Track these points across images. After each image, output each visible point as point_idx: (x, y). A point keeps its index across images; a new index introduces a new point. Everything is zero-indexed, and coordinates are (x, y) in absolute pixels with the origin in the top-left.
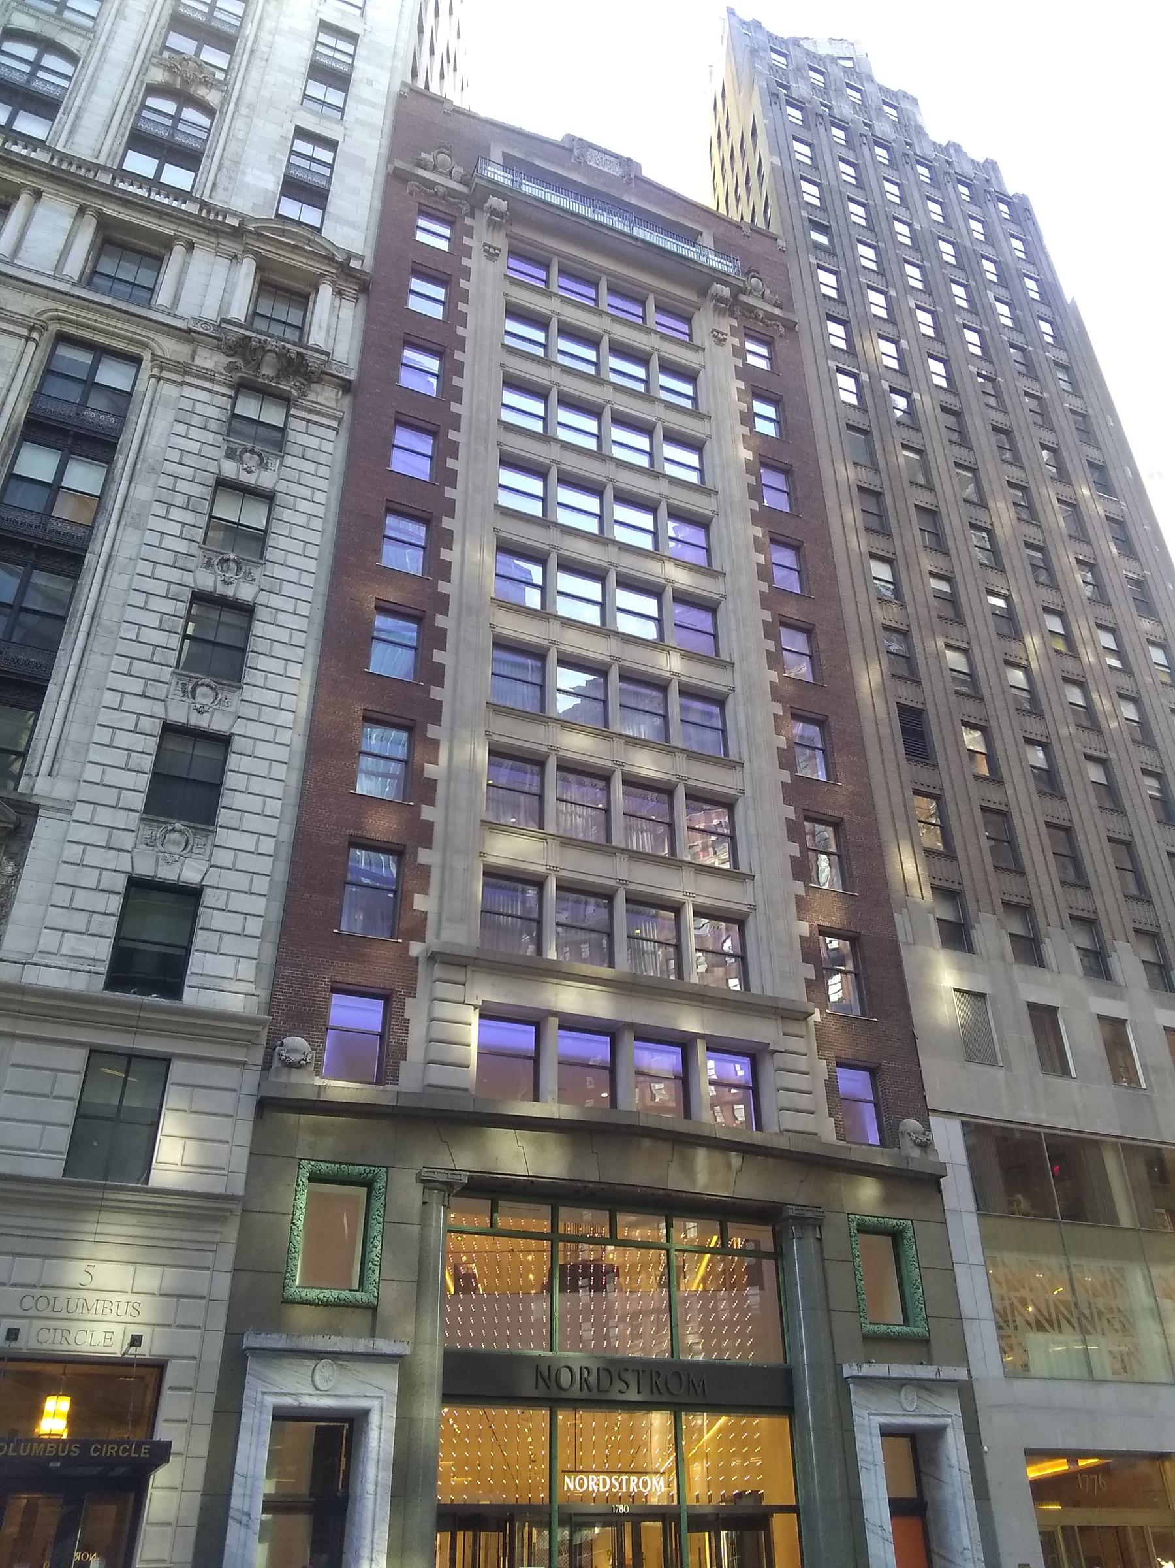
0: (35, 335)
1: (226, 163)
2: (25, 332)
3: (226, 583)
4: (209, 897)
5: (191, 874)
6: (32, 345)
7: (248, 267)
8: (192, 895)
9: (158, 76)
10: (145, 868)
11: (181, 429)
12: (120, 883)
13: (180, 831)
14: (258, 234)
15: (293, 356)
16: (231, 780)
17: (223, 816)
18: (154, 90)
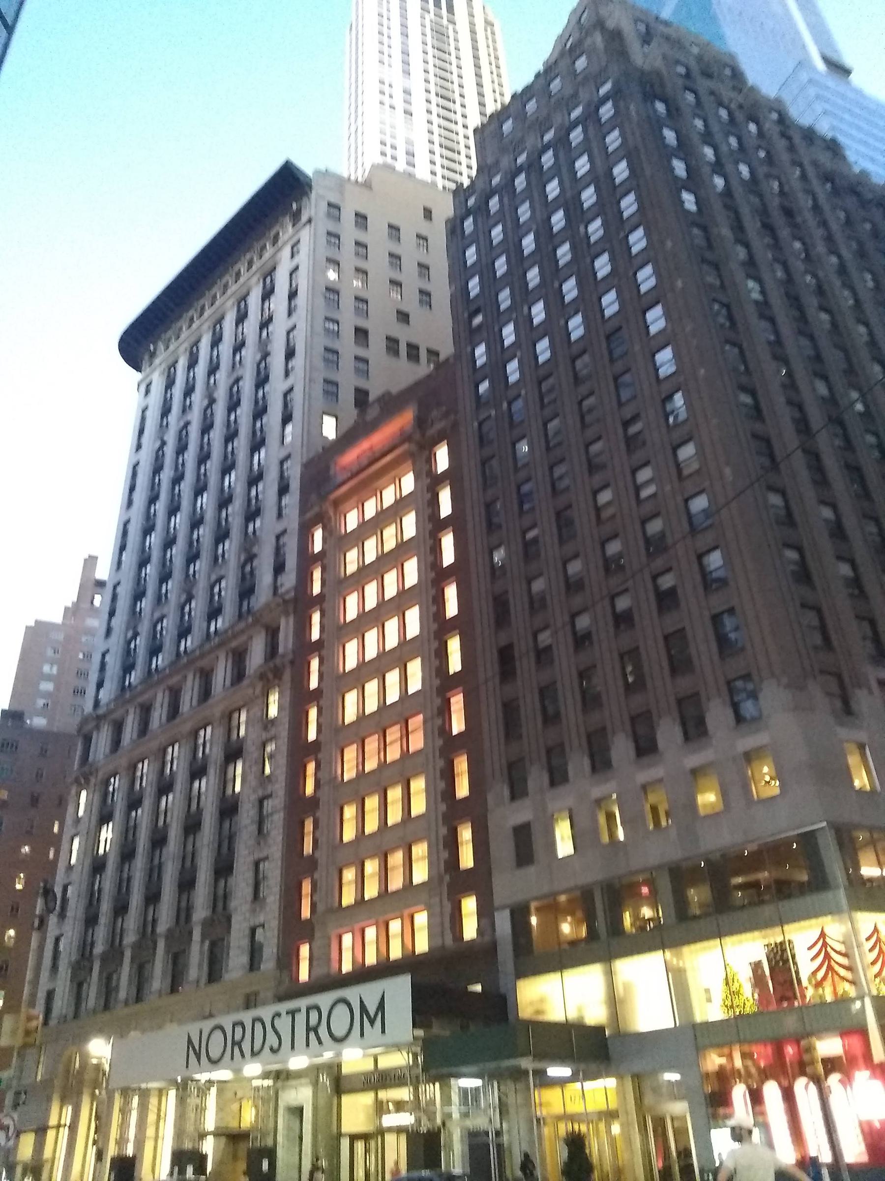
7: (263, 634)
9: (243, 558)
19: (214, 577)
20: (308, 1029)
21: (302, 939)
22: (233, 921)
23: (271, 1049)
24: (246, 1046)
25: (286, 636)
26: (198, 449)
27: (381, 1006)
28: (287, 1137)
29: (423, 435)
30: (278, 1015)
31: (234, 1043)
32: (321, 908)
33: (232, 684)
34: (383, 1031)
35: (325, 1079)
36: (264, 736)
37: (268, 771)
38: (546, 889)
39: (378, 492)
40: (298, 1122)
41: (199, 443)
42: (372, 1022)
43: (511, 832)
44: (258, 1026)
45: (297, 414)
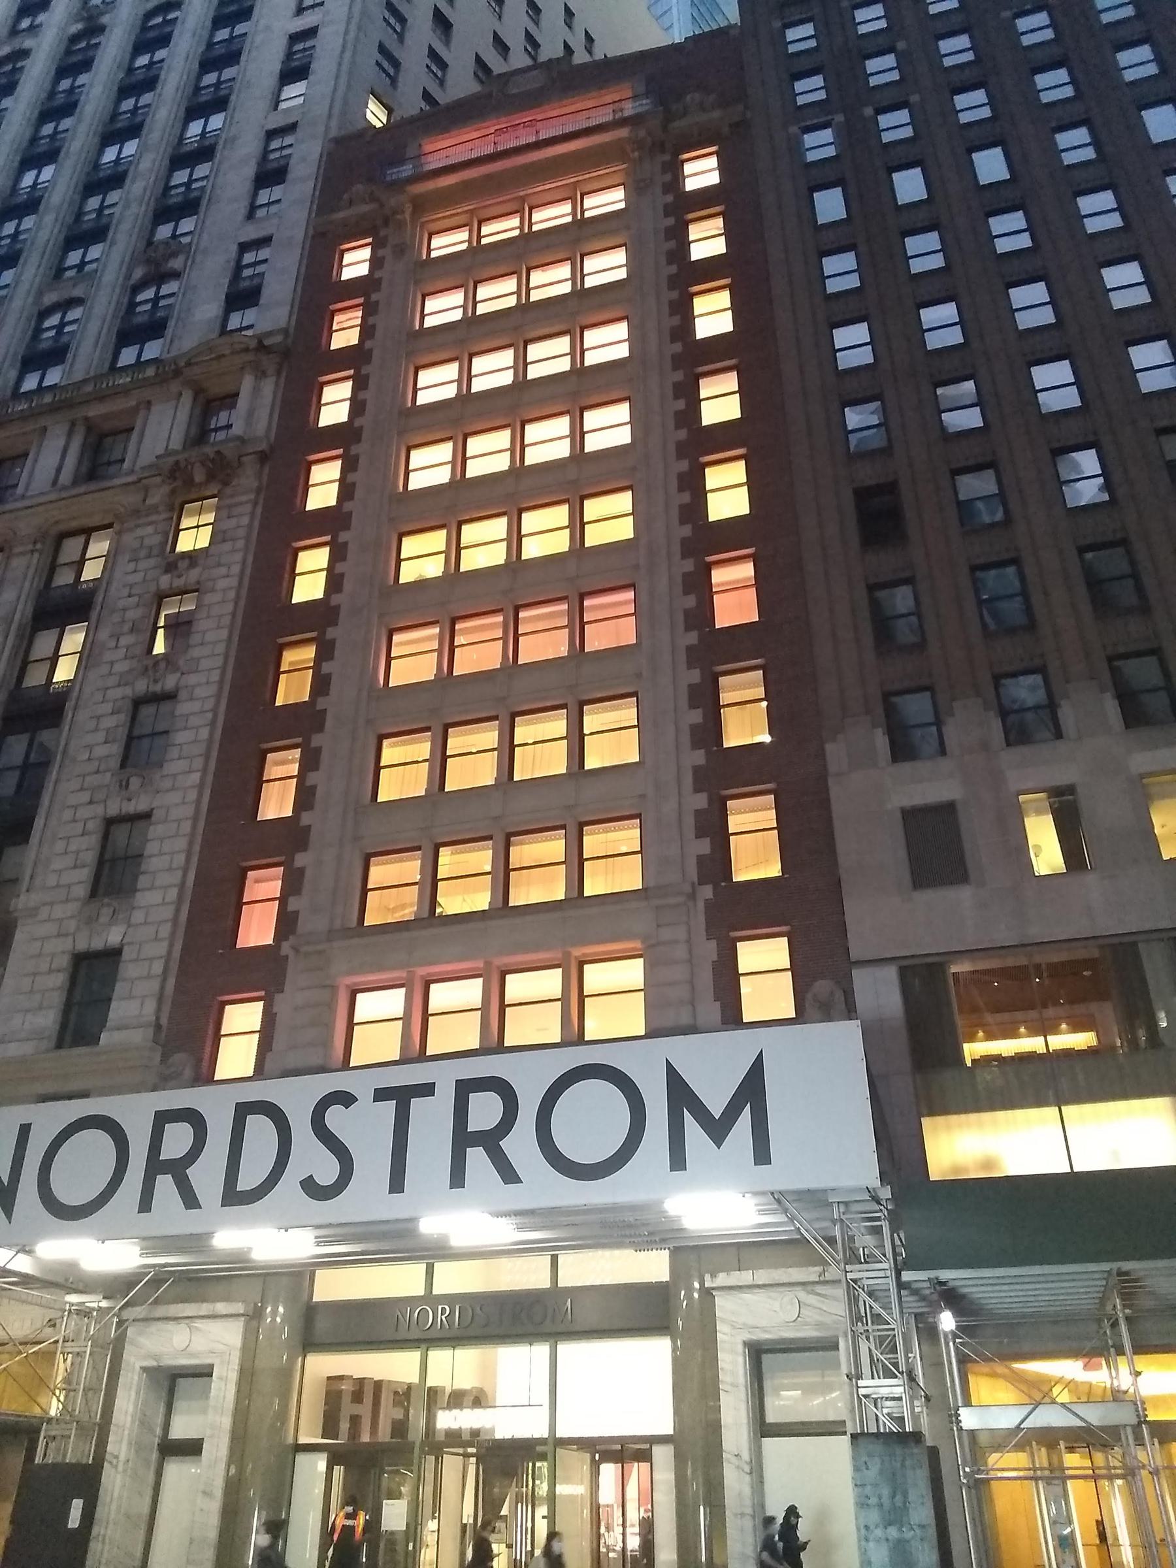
0: (39, 546)
1: (183, 315)
2: (30, 547)
3: (156, 681)
4: (127, 954)
5: (114, 937)
6: (36, 555)
8: (113, 955)
9: (138, 273)
10: (82, 946)
11: (132, 566)
12: (64, 961)
13: (109, 905)
14: (189, 364)
15: (212, 456)
16: (151, 848)
17: (143, 881)
18: (136, 289)
19: (50, 298)
20: (463, 1139)
21: (241, 991)
22: (19, 936)
23: (310, 1187)
24: (207, 1175)
25: (250, 414)
26: (44, 95)
27: (752, 1090)
28: (138, 1447)
29: (665, 128)
30: (345, 1099)
31: (155, 1166)
32: (308, 924)
33: (75, 482)
34: (762, 1154)
35: (277, 1314)
36: (165, 581)
37: (159, 648)
38: (1004, 936)
39: (523, 208)
40: (162, 1409)
41: (47, 86)
42: (718, 1130)
43: (899, 815)
44: (260, 1130)
45: (324, 64)
